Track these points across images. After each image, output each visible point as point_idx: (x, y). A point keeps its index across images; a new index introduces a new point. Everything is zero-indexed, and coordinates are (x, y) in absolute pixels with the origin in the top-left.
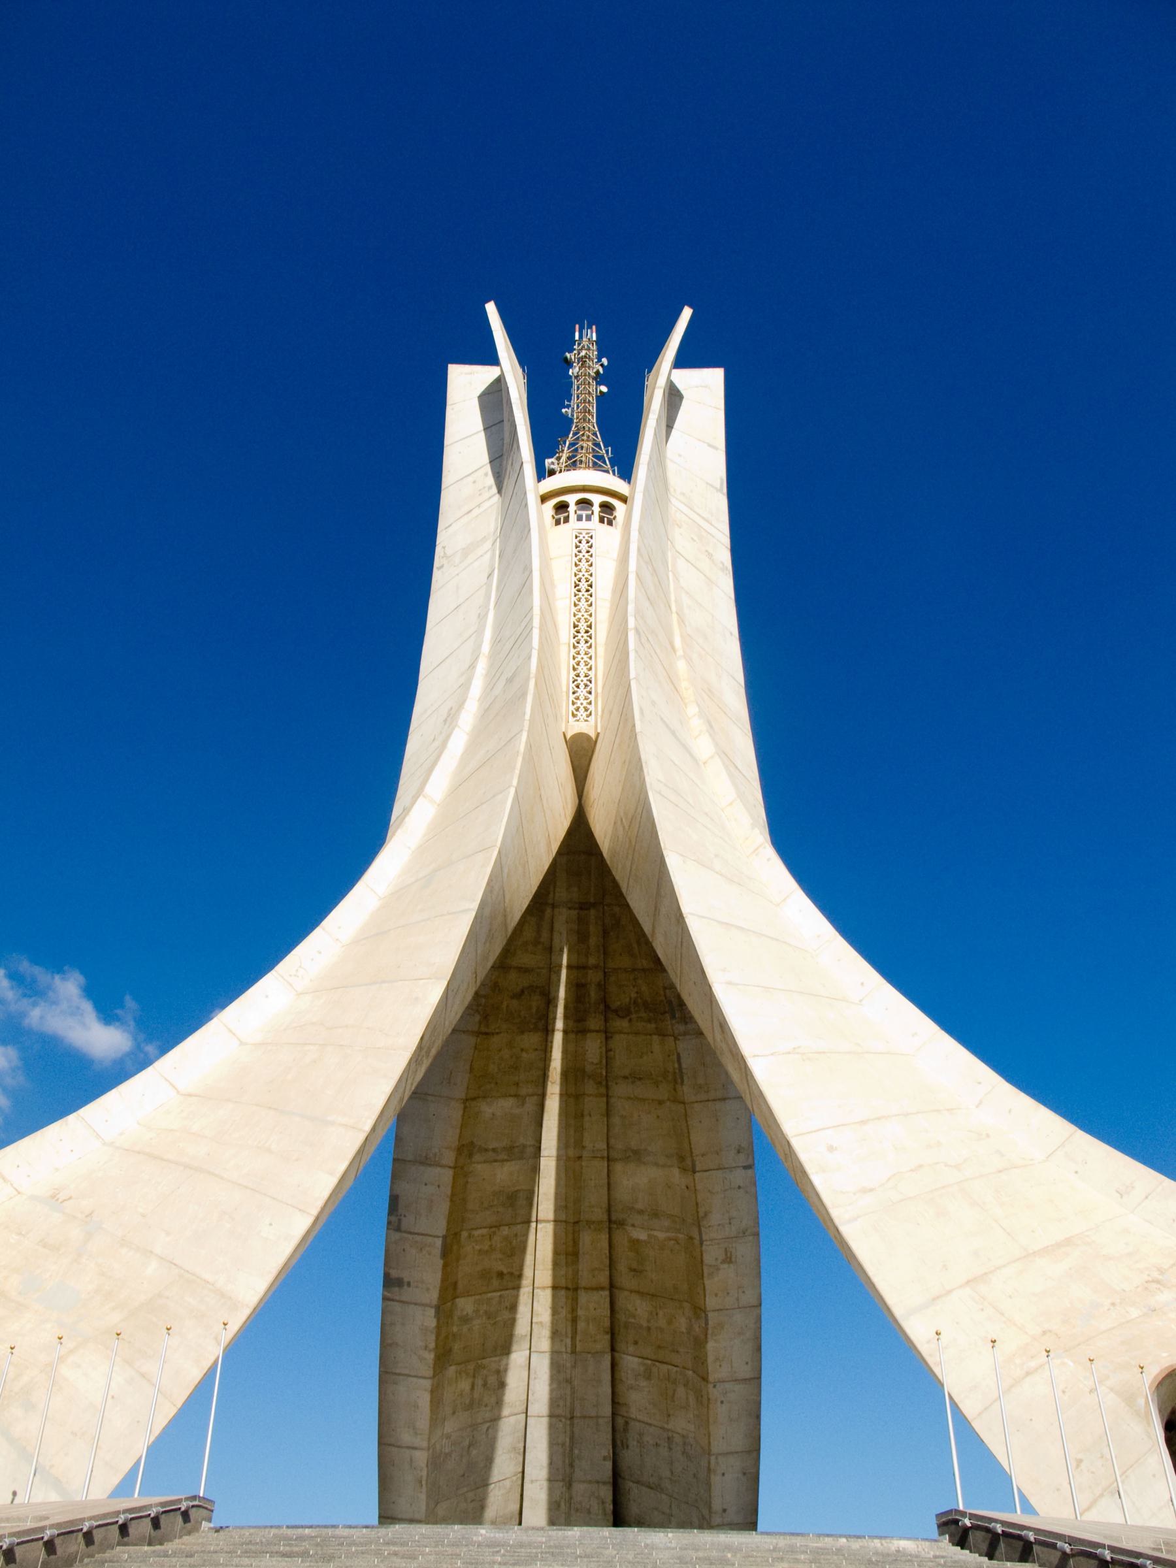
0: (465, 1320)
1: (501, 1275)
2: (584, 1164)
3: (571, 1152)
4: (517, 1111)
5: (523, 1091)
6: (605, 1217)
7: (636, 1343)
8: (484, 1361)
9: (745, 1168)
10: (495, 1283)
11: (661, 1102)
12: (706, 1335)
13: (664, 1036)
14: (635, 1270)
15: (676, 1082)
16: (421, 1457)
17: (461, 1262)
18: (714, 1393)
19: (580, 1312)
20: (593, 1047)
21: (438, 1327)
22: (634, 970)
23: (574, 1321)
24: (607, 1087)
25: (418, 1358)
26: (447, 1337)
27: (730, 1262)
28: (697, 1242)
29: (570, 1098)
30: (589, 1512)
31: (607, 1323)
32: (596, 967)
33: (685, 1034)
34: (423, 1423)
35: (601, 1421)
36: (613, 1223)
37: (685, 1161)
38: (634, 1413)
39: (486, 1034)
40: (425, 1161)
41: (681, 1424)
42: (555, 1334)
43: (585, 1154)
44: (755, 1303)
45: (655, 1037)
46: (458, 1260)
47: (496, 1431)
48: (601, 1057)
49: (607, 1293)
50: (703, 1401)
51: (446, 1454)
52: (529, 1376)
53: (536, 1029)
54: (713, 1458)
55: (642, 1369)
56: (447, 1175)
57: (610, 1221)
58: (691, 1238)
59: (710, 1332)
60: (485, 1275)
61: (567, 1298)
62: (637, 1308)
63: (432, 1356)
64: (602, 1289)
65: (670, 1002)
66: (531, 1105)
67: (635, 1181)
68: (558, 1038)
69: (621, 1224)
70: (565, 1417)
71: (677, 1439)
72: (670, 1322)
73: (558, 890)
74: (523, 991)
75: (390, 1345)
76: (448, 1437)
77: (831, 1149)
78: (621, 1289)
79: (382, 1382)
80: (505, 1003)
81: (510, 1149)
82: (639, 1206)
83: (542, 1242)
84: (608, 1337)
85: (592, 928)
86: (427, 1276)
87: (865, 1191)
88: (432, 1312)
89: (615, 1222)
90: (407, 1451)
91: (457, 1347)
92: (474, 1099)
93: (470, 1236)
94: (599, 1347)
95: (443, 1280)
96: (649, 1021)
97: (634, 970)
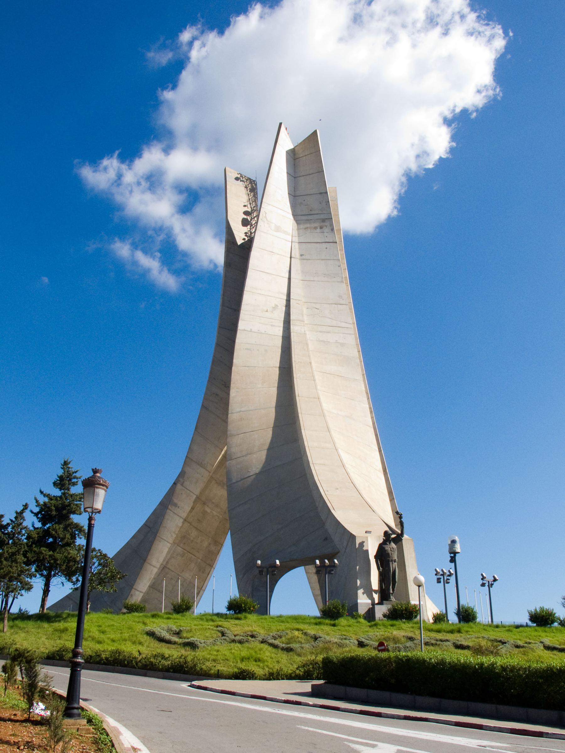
14: (199, 520)
40: (201, 465)
55: (182, 553)
63: (175, 536)
82: (213, 501)
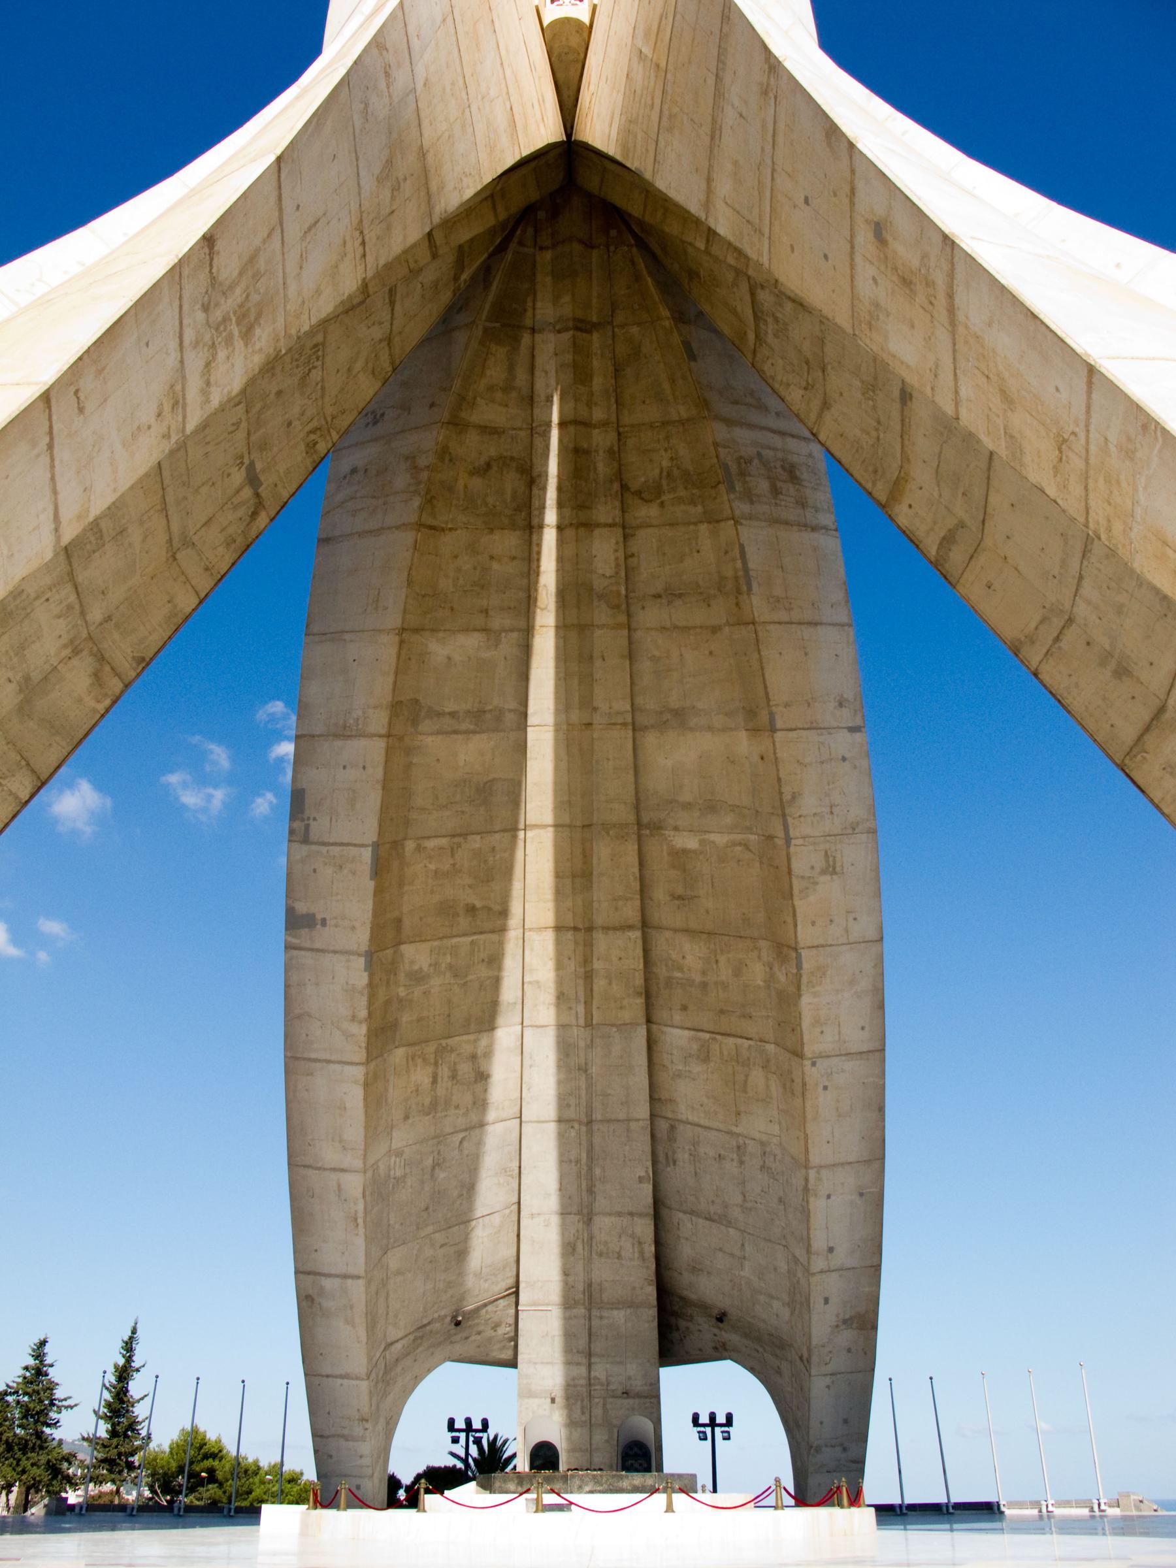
0: (418, 977)
1: (471, 910)
2: (595, 735)
3: (575, 716)
4: (486, 655)
5: (496, 622)
6: (632, 818)
7: (684, 1008)
8: (449, 1041)
9: (853, 730)
10: (464, 922)
11: (715, 630)
12: (799, 988)
13: (718, 522)
14: (680, 898)
15: (739, 592)
16: (354, 1184)
17: (406, 888)
18: (813, 1074)
19: (597, 965)
20: (604, 550)
21: (371, 985)
22: (664, 424)
23: (589, 977)
24: (629, 615)
25: (342, 1034)
26: (388, 1003)
27: (834, 872)
28: (780, 842)
29: (572, 629)
30: (619, 1257)
31: (639, 981)
32: (604, 424)
33: (750, 517)
34: (355, 1132)
35: (633, 1125)
36: (644, 826)
37: (758, 717)
38: (684, 1112)
39: (432, 528)
40: (344, 732)
41: (760, 1124)
42: (561, 998)
43: (597, 719)
44: (872, 934)
45: (703, 527)
46: (401, 885)
47: (480, 1143)
48: (617, 565)
49: (638, 934)
50: (794, 1088)
51: (397, 1179)
52: (526, 1062)
53: (513, 526)
54: (812, 1174)
55: (695, 1047)
56: (376, 749)
57: (639, 824)
58: (771, 838)
59: (804, 980)
60: (447, 910)
61: (576, 943)
62: (687, 956)
63: (364, 1029)
64: (630, 927)
65: (726, 467)
66: (508, 645)
67: (676, 758)
68: (549, 539)
69: (657, 827)
70: (581, 1121)
71: (752, 1147)
72: (737, 973)
73: (539, 304)
74: (488, 466)
75: (299, 1017)
76: (399, 1154)
78: (659, 928)
79: (288, 1072)
80: (460, 484)
81: (478, 715)
82: (687, 797)
83: (536, 860)
84: (640, 1001)
85: (596, 363)
86: (350, 908)
88: (361, 962)
89: (648, 826)
90: (334, 1176)
91: (405, 1018)
92: (417, 631)
93: (419, 849)
94: (626, 1016)
95: (378, 913)
96: (693, 503)
97: (664, 424)
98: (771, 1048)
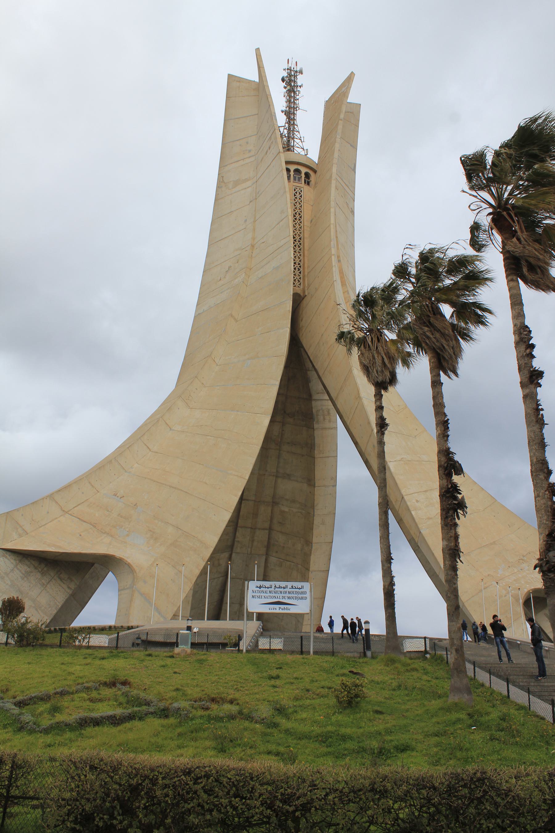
7: (277, 552)
11: (303, 456)
14: (280, 523)
23: (253, 541)
31: (266, 543)
36: (274, 503)
57: (273, 502)
58: (309, 513)
62: (280, 539)
64: (266, 529)
67: (286, 487)
77: (417, 501)
84: (265, 549)
87: (429, 518)
98: (300, 566)
